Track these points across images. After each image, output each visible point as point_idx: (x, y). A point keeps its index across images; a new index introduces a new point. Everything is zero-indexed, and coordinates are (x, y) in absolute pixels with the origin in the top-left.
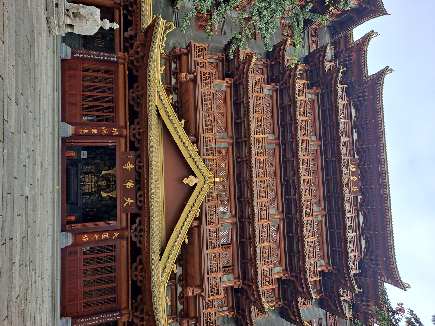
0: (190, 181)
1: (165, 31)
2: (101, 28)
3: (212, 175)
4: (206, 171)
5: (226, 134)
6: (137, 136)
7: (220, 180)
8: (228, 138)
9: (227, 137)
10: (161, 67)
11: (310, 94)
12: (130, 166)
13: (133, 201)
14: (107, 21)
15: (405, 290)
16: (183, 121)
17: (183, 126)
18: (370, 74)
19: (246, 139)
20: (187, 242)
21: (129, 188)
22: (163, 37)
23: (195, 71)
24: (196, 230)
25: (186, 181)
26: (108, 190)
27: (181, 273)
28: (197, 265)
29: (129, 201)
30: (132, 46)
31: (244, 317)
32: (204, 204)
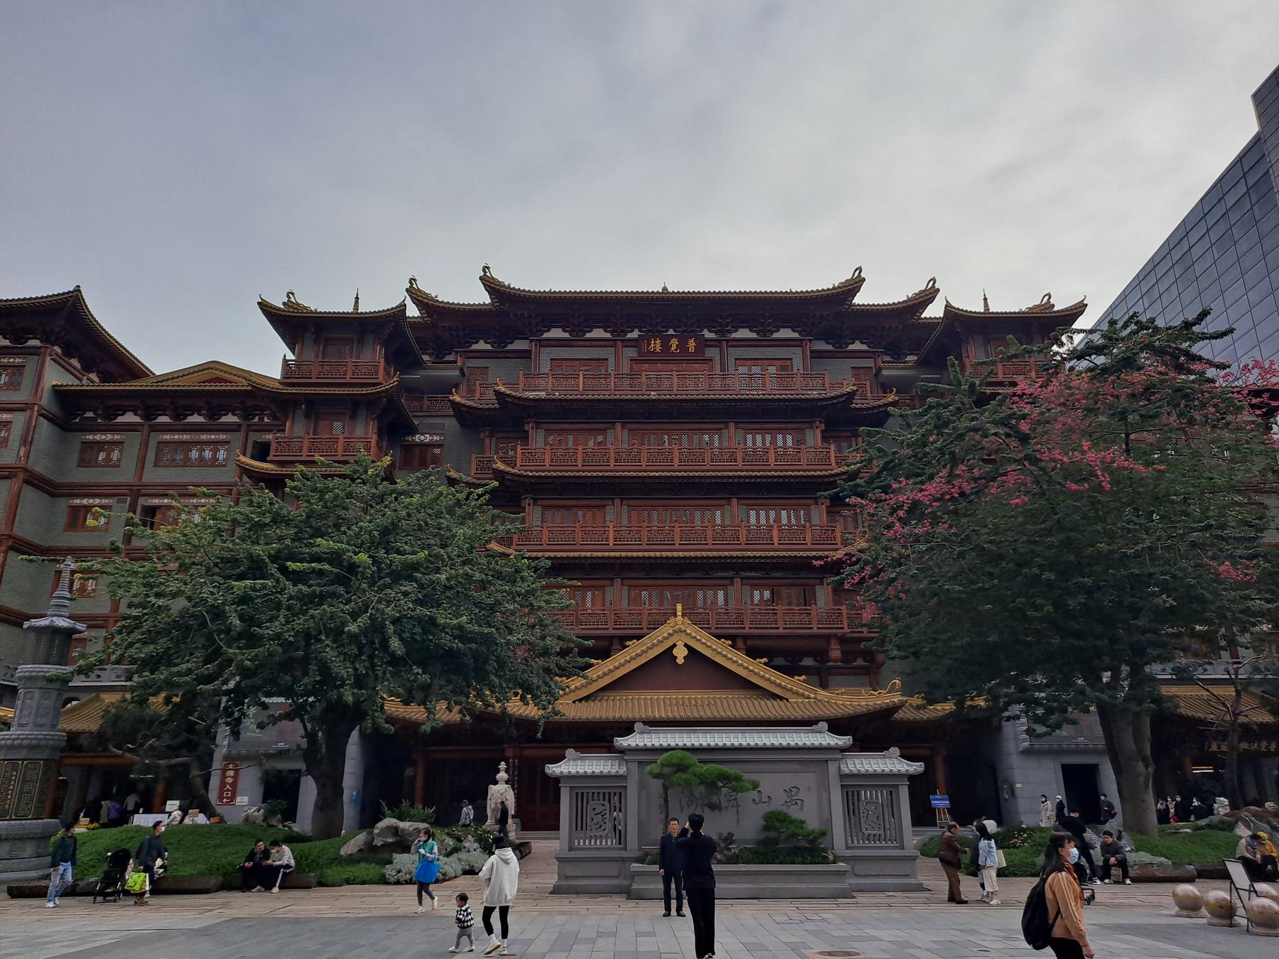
0: (680, 654)
2: (507, 782)
3: (672, 620)
4: (665, 630)
7: (679, 607)
14: (499, 776)
15: (864, 280)
18: (488, 301)
20: (765, 660)
24: (750, 643)
25: (680, 661)
32: (713, 630)
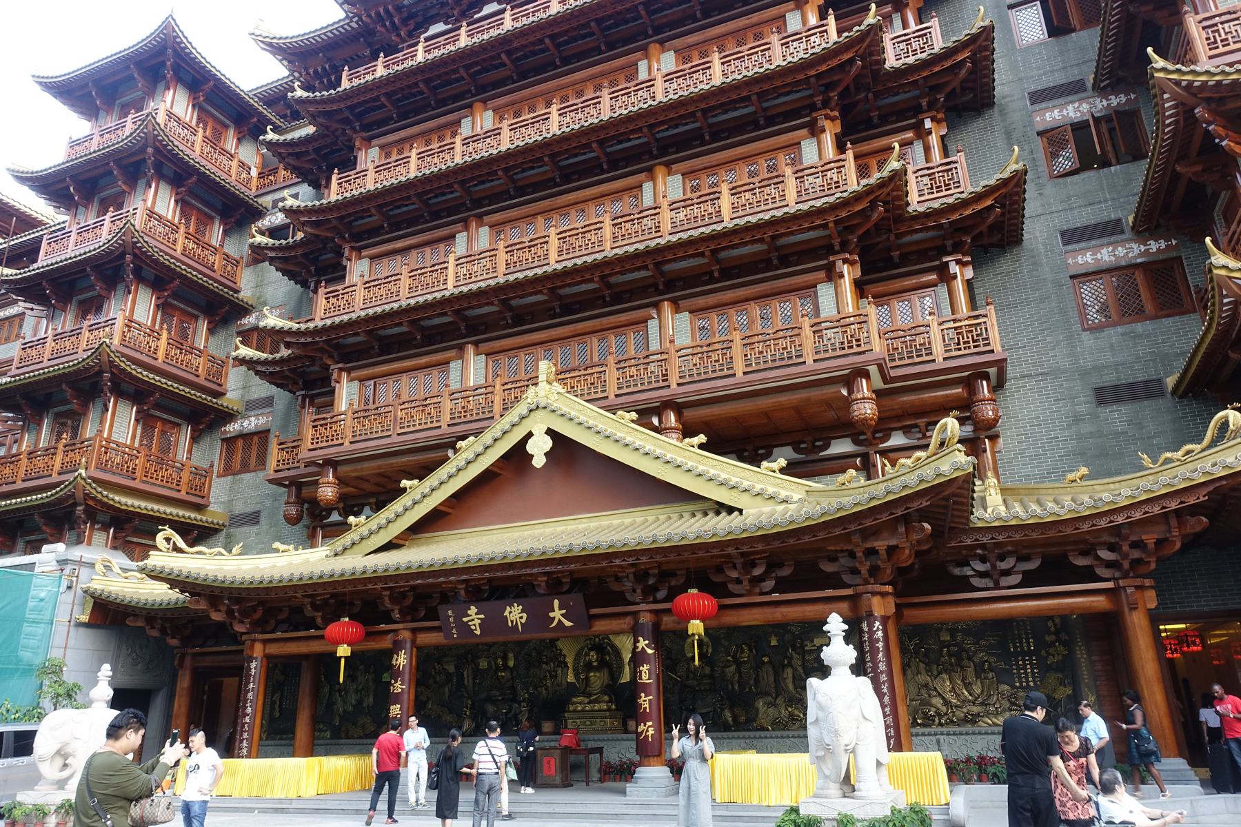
0: (539, 448)
1: (180, 551)
5: (452, 365)
6: (758, 571)
8: (462, 358)
9: (460, 361)
10: (277, 551)
11: (368, 158)
12: (474, 617)
13: (556, 603)
16: (405, 483)
17: (416, 482)
19: (448, 309)
20: (702, 438)
21: (525, 615)
22: (197, 553)
23: (314, 463)
25: (539, 461)
26: (615, 666)
27: (848, 440)
28: (783, 398)
29: (557, 614)
30: (221, 626)
31: (960, 227)
32: (612, 399)
